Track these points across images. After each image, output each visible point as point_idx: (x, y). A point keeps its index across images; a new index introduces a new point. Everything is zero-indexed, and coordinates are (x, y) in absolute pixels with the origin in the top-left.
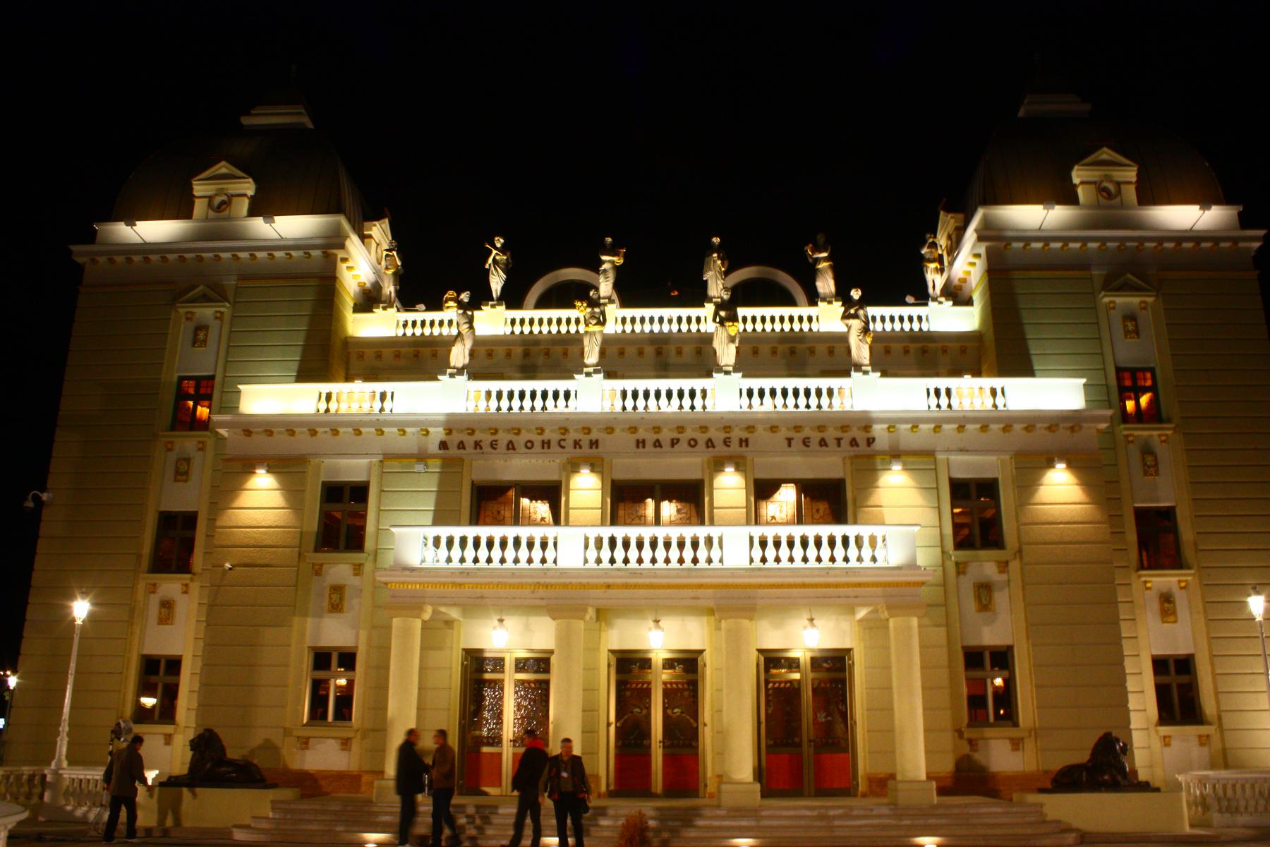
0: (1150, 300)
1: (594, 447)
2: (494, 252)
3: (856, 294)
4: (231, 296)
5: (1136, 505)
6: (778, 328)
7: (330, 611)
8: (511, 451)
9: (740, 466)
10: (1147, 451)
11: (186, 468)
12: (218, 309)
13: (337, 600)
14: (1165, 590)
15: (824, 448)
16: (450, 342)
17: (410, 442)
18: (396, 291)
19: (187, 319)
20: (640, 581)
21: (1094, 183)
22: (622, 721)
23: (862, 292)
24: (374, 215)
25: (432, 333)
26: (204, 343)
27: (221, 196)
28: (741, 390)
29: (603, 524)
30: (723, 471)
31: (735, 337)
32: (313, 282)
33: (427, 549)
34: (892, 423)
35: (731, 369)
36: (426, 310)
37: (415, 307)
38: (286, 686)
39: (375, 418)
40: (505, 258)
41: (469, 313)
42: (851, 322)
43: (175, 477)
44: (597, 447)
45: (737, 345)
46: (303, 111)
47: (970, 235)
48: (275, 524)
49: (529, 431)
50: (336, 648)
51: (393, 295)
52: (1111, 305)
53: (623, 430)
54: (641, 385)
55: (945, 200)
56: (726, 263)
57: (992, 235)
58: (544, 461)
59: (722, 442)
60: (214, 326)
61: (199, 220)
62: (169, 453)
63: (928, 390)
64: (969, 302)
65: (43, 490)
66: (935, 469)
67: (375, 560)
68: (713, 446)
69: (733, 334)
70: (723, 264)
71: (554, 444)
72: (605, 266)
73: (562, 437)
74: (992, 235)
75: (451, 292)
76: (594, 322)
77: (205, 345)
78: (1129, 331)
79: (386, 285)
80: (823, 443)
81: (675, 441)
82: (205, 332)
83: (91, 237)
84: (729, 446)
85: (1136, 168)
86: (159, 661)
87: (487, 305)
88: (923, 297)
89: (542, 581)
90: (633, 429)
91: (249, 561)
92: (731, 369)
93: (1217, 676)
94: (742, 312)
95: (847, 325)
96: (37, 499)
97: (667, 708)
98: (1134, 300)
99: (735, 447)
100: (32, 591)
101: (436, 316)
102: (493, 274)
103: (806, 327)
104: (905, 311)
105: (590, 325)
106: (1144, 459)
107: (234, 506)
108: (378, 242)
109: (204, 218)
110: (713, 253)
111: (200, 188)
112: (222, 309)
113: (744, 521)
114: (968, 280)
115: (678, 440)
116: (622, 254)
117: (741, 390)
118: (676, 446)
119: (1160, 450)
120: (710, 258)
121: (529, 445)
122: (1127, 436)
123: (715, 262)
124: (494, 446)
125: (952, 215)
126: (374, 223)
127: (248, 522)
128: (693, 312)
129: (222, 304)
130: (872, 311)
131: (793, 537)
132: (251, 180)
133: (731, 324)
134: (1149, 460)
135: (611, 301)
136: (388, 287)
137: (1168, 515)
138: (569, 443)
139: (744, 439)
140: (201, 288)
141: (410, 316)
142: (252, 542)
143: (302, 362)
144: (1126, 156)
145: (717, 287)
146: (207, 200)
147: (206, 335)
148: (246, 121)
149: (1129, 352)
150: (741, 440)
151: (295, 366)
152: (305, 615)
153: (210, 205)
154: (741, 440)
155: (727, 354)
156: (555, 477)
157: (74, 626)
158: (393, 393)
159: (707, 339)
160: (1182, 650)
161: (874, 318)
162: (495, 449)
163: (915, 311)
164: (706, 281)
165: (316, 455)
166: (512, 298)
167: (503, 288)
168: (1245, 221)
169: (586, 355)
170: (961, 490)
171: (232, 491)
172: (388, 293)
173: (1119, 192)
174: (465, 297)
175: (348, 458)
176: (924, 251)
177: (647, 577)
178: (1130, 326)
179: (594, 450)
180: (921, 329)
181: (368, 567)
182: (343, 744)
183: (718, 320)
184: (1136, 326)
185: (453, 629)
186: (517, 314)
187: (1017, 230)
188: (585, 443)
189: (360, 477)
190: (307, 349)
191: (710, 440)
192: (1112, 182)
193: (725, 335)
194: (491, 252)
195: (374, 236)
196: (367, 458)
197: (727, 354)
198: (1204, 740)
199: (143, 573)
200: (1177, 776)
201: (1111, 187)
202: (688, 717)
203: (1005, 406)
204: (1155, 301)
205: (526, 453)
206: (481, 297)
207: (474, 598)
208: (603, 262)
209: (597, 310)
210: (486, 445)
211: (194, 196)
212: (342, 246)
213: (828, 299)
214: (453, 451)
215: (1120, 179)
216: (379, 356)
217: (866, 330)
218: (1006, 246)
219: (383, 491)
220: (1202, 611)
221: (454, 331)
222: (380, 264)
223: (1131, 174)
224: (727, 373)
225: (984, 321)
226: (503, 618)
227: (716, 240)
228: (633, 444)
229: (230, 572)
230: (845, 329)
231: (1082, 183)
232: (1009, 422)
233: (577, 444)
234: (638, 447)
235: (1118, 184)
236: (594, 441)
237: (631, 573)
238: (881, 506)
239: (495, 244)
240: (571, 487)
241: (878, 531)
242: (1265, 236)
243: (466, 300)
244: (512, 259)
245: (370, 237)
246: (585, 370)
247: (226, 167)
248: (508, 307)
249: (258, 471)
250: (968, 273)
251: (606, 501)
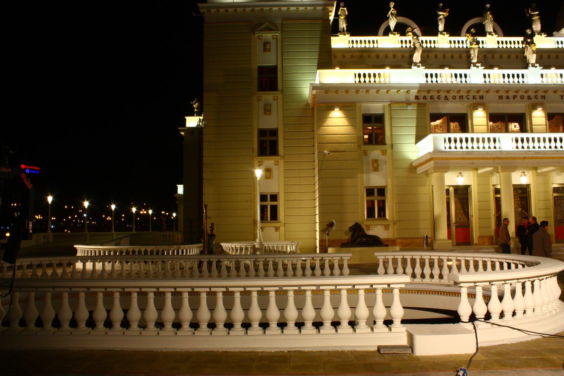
1: (481, 99)
6: (505, 47)
7: (373, 171)
8: (447, 100)
9: (483, 106)
11: (269, 108)
12: (274, 34)
13: (376, 166)
16: (413, 50)
17: (402, 95)
18: (347, 27)
19: (259, 39)
20: (539, 156)
22: (498, 214)
29: (488, 132)
30: (334, 110)
32: (319, 22)
37: (337, 34)
38: (358, 204)
40: (396, 12)
43: (265, 112)
44: (483, 99)
48: (345, 133)
49: (454, 92)
50: (376, 187)
51: (345, 28)
53: (493, 92)
54: (511, 72)
58: (460, 105)
59: (534, 97)
60: (273, 42)
62: (260, 102)
67: (392, 148)
68: (531, 99)
70: (492, 16)
71: (464, 97)
72: (441, 17)
73: (468, 94)
76: (475, 43)
77: (270, 51)
81: (515, 97)
82: (269, 45)
84: (537, 99)
86: (267, 195)
89: (499, 156)
90: (497, 92)
99: (539, 99)
100: (204, 166)
102: (391, 19)
103: (433, 45)
107: (323, 125)
110: (488, 12)
112: (276, 34)
113: (545, 131)
115: (516, 96)
116: (447, 11)
118: (515, 99)
120: (486, 14)
121: (454, 98)
123: (489, 16)
124: (439, 98)
127: (332, 133)
129: (278, 32)
131: (462, 138)
136: (343, 24)
138: (471, 97)
142: (335, 141)
143: (319, 59)
147: (270, 46)
150: (542, 96)
151: (316, 61)
152: (362, 172)
154: (542, 96)
155: (532, 58)
156: (464, 112)
157: (257, 180)
162: (440, 99)
164: (484, 24)
165: (360, 102)
171: (322, 118)
175: (374, 103)
177: (491, 154)
179: (481, 100)
181: (389, 151)
182: (385, 227)
185: (429, 177)
186: (404, 38)
188: (478, 97)
189: (381, 112)
191: (529, 96)
193: (531, 50)
196: (383, 103)
199: (256, 156)
205: (453, 101)
207: (470, 164)
208: (440, 15)
210: (435, 97)
214: (421, 100)
216: (344, 57)
219: (392, 118)
226: (461, 172)
227: (488, 6)
228: (498, 97)
229: (328, 155)
233: (474, 97)
234: (500, 99)
236: (481, 96)
237: (536, 153)
240: (474, 116)
248: (351, 36)
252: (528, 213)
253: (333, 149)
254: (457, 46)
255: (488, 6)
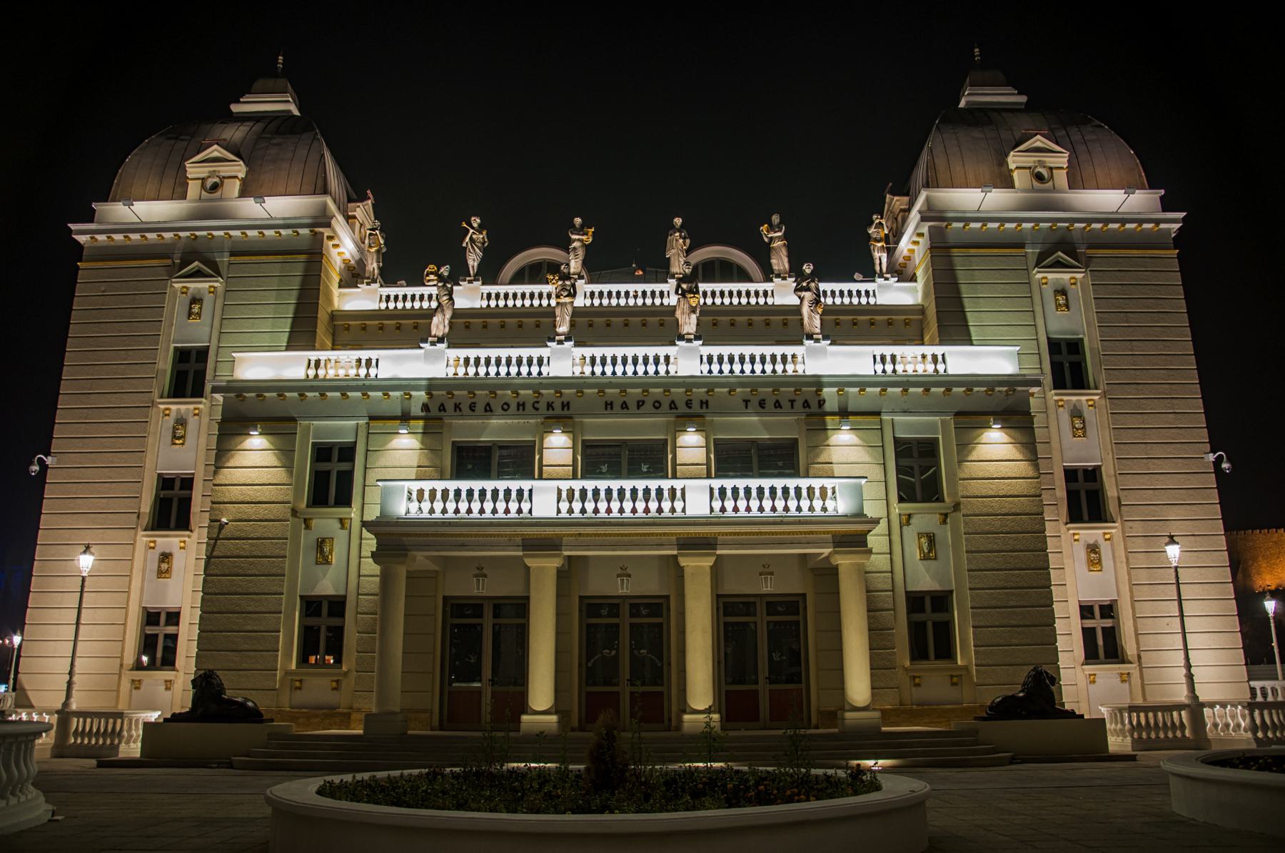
0: (1079, 276)
1: (566, 408)
2: (471, 231)
3: (808, 269)
4: (224, 270)
5: (1065, 464)
8: (489, 413)
10: (1076, 413)
14: (1091, 542)
15: (779, 410)
16: (430, 314)
18: (380, 268)
21: (1030, 168)
23: (813, 265)
24: (356, 195)
25: (413, 306)
26: (199, 315)
27: (214, 177)
28: (701, 356)
29: (574, 477)
31: (696, 307)
32: (303, 258)
33: (412, 501)
34: (842, 383)
35: (692, 337)
36: (407, 286)
39: (360, 383)
40: (481, 236)
41: (449, 286)
42: (803, 294)
43: (172, 441)
45: (698, 315)
46: (290, 99)
47: (914, 216)
51: (376, 271)
52: (1044, 281)
55: (891, 184)
56: (688, 241)
57: (932, 214)
60: (208, 299)
61: (195, 201)
63: (874, 357)
64: (913, 279)
65: (48, 454)
66: (881, 429)
69: (694, 305)
70: (684, 243)
72: (576, 244)
73: (536, 400)
74: (932, 214)
75: (431, 266)
76: (565, 294)
78: (1060, 305)
79: (370, 262)
80: (778, 405)
81: (641, 403)
83: (90, 217)
85: (1067, 155)
87: (465, 281)
88: (870, 275)
91: (245, 517)
92: (692, 337)
93: (1138, 619)
94: (703, 287)
95: (799, 297)
96: (41, 462)
97: (634, 649)
98: (1064, 277)
99: (696, 408)
101: (418, 291)
102: (470, 252)
104: (854, 287)
105: (561, 297)
106: (1073, 422)
108: (361, 222)
109: (198, 198)
110: (675, 232)
111: (194, 170)
112: (216, 284)
114: (912, 258)
115: (643, 402)
116: (590, 233)
117: (701, 356)
118: (641, 408)
119: (1088, 413)
121: (506, 407)
122: (1057, 401)
125: (898, 198)
126: (358, 204)
128: (658, 287)
130: (823, 286)
132: (241, 163)
133: (692, 295)
135: (581, 277)
136: (372, 264)
137: (1093, 474)
138: (542, 406)
139: (704, 401)
140: (196, 263)
141: (392, 291)
144: (1057, 144)
145: (679, 265)
146: (201, 181)
147: (201, 308)
148: (235, 108)
149: (1061, 324)
153: (203, 186)
155: (689, 324)
158: (377, 360)
159: (671, 311)
160: (1106, 598)
161: (825, 292)
163: (863, 287)
164: (669, 258)
166: (489, 273)
167: (479, 265)
168: (1166, 205)
169: (558, 324)
170: (904, 448)
172: (372, 269)
173: (1052, 177)
174: (445, 271)
176: (871, 231)
178: (1061, 300)
180: (868, 303)
183: (680, 292)
184: (1067, 299)
186: (494, 289)
187: (957, 211)
188: (557, 405)
190: (296, 320)
192: (1044, 167)
193: (686, 306)
194: (468, 231)
195: (357, 216)
197: (689, 324)
198: (1125, 678)
200: (1100, 708)
201: (1045, 172)
202: (654, 658)
203: (945, 371)
204: (1083, 277)
206: (459, 273)
209: (568, 283)
211: (188, 178)
212: (329, 225)
213: (782, 275)
214: (435, 412)
215: (1052, 165)
217: (817, 302)
218: (946, 227)
220: (1125, 560)
221: (434, 304)
222: (364, 243)
223: (1062, 160)
224: (689, 341)
225: (926, 295)
227: (678, 221)
230: (796, 301)
231: (1017, 168)
232: (949, 383)
233: (550, 406)
235: (1051, 169)
238: (831, 463)
239: (471, 224)
241: (828, 483)
242: (1184, 219)
243: (446, 274)
244: (488, 238)
245: (354, 217)
246: (557, 338)
247: (218, 151)
249: (251, 433)
250: (912, 251)
251: (577, 459)
252: (661, 659)
253: (239, 516)
254: (614, 302)
255: (678, 221)
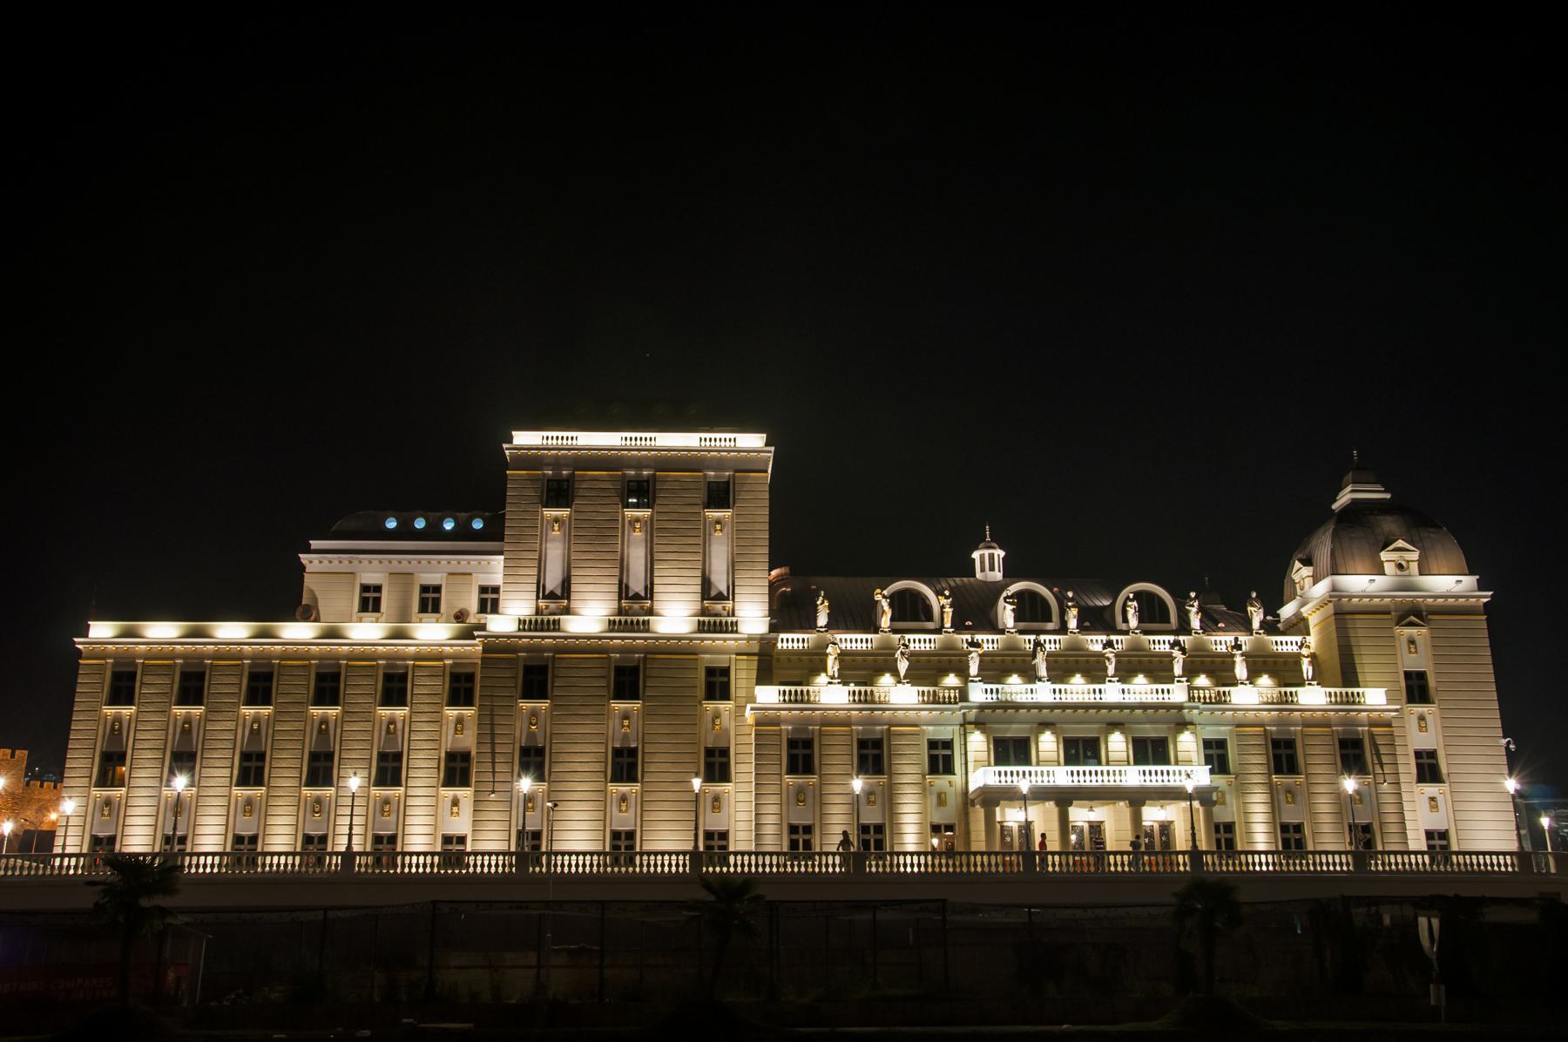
98: (1413, 631)
134: (1423, 724)
137: (1432, 754)
144: (1414, 546)
160: (1442, 827)
168: (1481, 586)
173: (1408, 568)
184: (1416, 648)
201: (1404, 563)
223: (1415, 556)
231: (1387, 561)
235: (1408, 561)
242: (1492, 596)
